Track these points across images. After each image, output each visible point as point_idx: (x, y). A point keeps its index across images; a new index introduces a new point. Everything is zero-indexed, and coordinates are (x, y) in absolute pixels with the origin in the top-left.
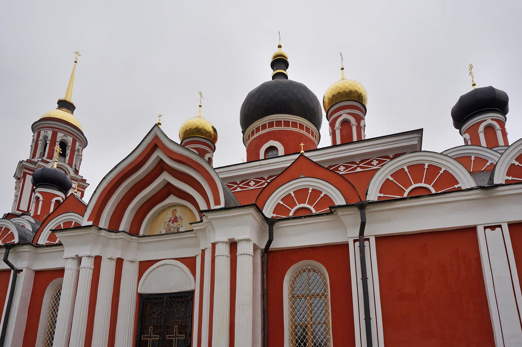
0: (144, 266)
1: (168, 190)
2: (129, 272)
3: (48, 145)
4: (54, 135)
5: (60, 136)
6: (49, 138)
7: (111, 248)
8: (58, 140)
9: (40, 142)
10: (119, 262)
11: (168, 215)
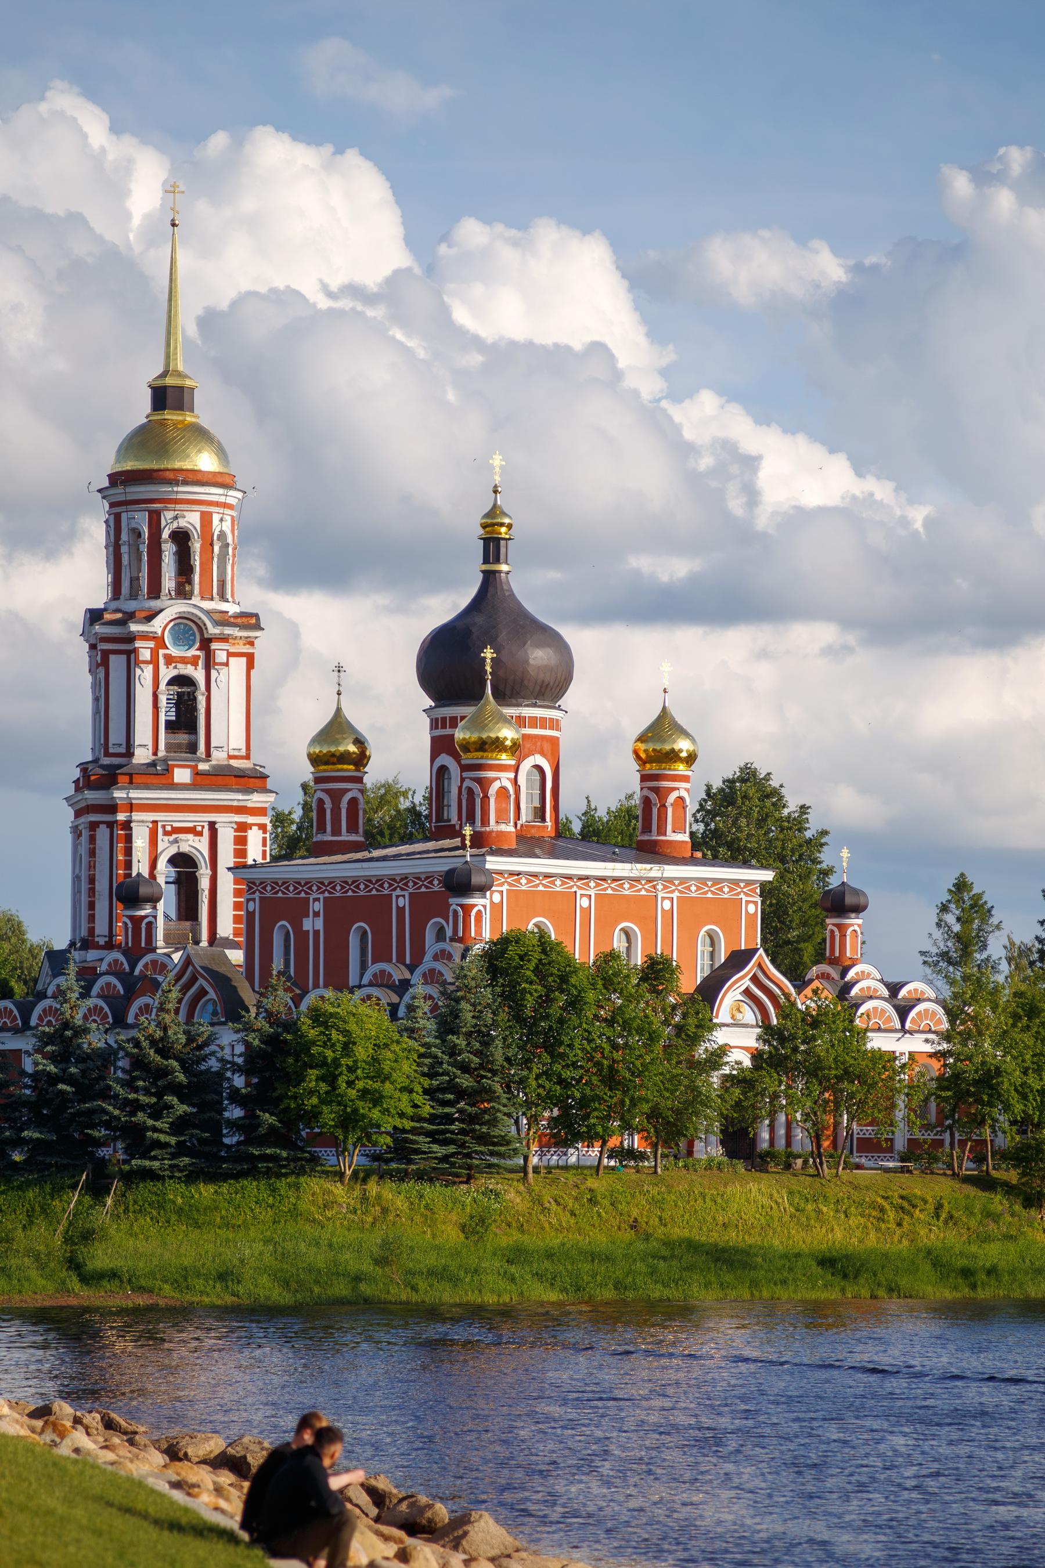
4: (155, 520)
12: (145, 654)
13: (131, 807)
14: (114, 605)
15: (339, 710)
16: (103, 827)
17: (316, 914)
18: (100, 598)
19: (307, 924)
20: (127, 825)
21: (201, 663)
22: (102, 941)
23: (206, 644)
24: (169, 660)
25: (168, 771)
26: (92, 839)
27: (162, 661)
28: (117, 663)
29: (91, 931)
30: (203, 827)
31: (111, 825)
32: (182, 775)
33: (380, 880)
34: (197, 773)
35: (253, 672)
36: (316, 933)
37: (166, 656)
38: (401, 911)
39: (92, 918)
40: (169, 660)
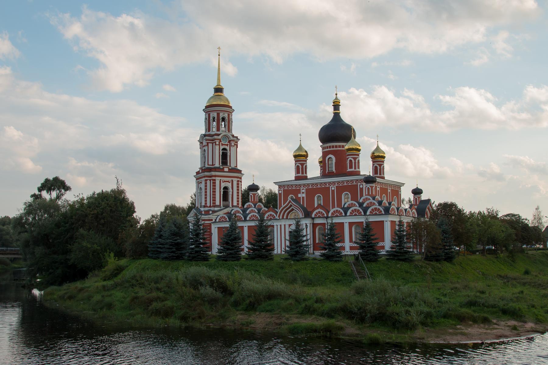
0: (290, 225)
1: (293, 210)
2: (287, 227)
4: (218, 114)
5: (221, 115)
6: (216, 118)
7: (283, 223)
8: (221, 118)
10: (285, 225)
11: (294, 214)
12: (217, 143)
13: (215, 176)
14: (208, 133)
15: (300, 145)
17: (303, 193)
18: (203, 132)
19: (299, 195)
20: (215, 180)
23: (230, 141)
24: (222, 145)
25: (223, 169)
26: (206, 183)
28: (210, 145)
29: (206, 203)
31: (210, 180)
32: (226, 169)
33: (325, 183)
34: (229, 169)
36: (303, 198)
38: (333, 191)
39: (206, 201)
40: (222, 145)
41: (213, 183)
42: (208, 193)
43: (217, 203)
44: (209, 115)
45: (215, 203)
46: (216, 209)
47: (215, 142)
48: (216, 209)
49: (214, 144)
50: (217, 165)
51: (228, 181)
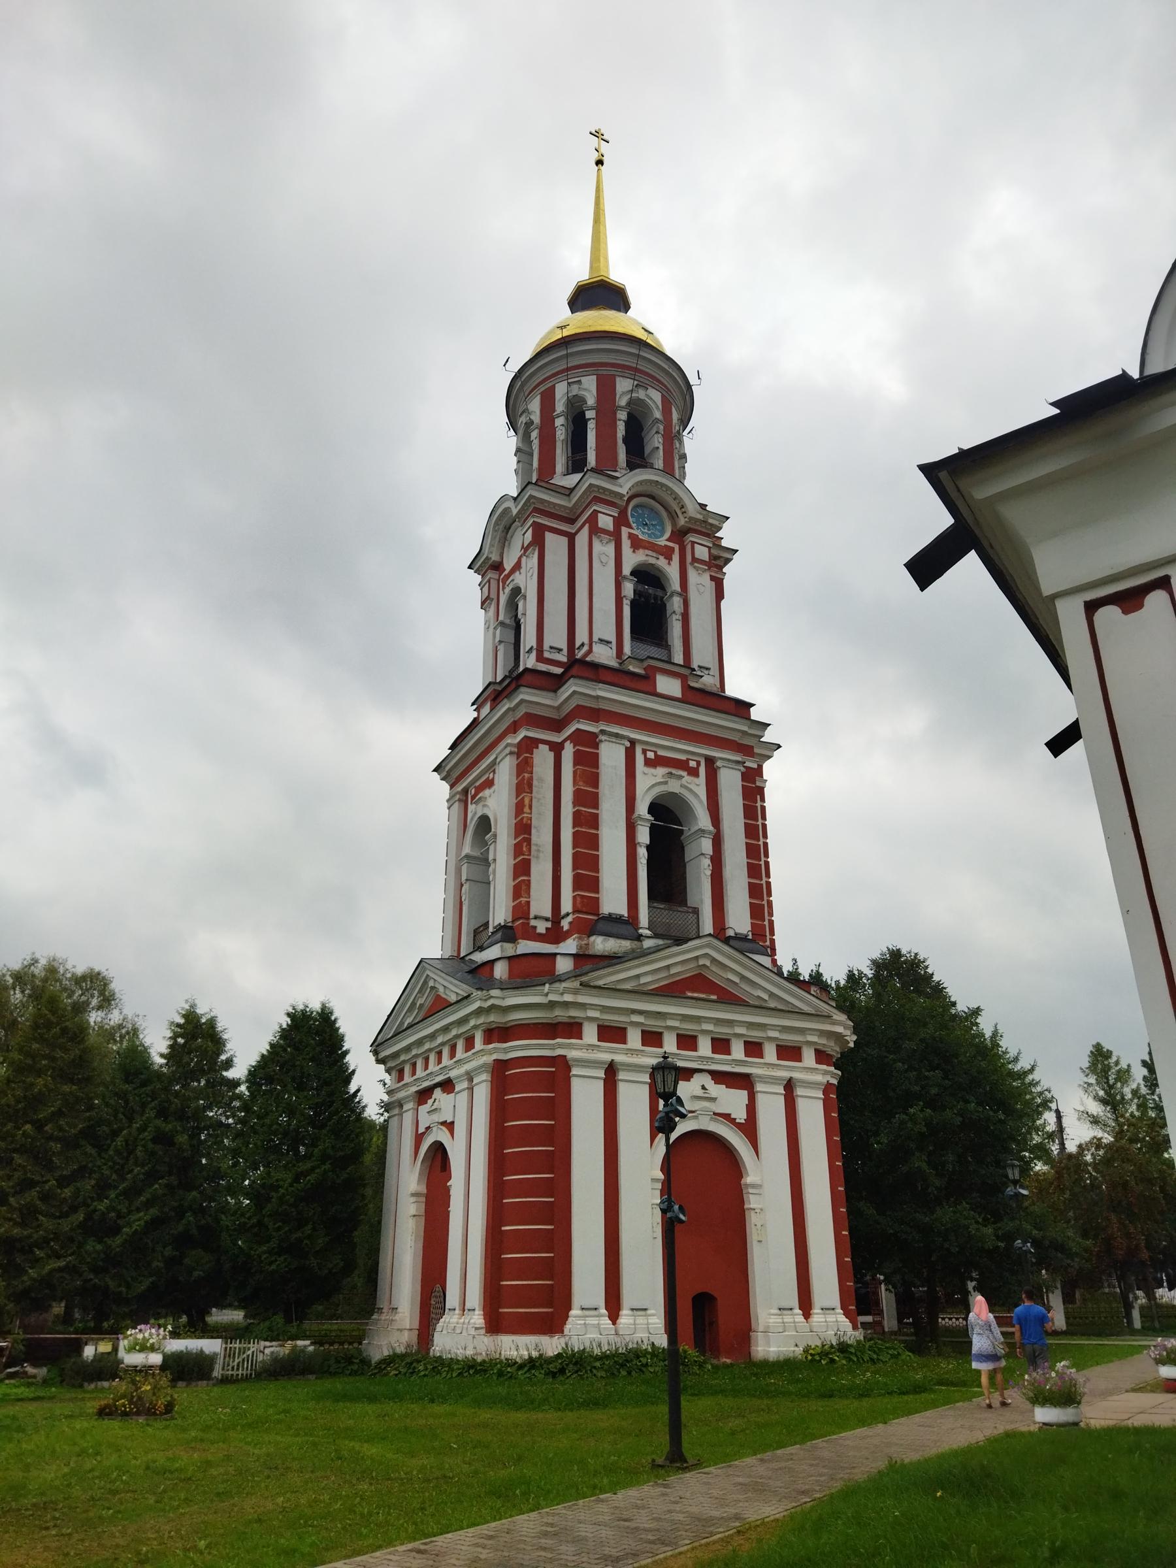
3: (591, 425)
6: (591, 401)
9: (559, 422)
16: (544, 748)
21: (676, 557)
22: (542, 927)
23: (679, 535)
27: (626, 544)
28: (555, 545)
30: (698, 763)
31: (557, 748)
32: (668, 685)
34: (686, 688)
35: (723, 603)
37: (631, 536)
39: (521, 889)
41: (578, 759)
42: (542, 836)
43: (613, 900)
44: (548, 399)
45: (593, 905)
46: (601, 944)
47: (593, 520)
48: (601, 944)
49: (582, 539)
50: (604, 655)
51: (682, 765)
